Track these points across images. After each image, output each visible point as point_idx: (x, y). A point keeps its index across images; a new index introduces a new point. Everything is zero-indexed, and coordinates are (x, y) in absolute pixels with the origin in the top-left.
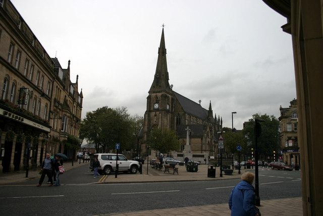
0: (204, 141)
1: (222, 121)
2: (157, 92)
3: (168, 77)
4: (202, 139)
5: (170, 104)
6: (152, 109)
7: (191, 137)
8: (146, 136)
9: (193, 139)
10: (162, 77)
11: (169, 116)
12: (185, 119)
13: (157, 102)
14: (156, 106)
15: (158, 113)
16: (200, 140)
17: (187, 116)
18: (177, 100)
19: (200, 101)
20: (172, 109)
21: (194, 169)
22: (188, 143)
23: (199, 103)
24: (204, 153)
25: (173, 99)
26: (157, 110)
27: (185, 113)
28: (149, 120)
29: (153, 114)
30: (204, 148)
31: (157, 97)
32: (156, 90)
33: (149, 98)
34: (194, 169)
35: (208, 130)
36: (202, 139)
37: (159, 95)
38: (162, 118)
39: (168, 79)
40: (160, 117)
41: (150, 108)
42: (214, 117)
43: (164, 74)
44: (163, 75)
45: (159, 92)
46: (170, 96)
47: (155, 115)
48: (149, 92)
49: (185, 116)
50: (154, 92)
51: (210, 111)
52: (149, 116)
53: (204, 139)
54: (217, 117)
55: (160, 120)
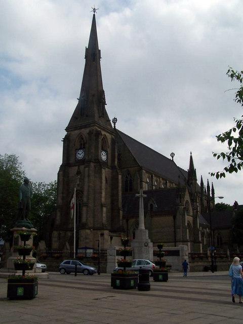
2: (81, 128)
3: (104, 99)
4: (175, 218)
5: (109, 150)
6: (72, 161)
7: (150, 213)
8: (59, 214)
9: (156, 219)
11: (105, 172)
12: (141, 181)
13: (82, 147)
14: (80, 155)
15: (82, 167)
16: (171, 218)
17: (146, 178)
18: (122, 142)
19: (173, 155)
20: (113, 161)
22: (142, 226)
23: (170, 158)
24: (180, 246)
25: (113, 142)
26: (82, 162)
27: (141, 169)
29: (73, 170)
30: (180, 236)
33: (66, 140)
35: (187, 197)
36: (175, 218)
37: (85, 131)
39: (104, 103)
40: (86, 174)
42: (199, 182)
44: (93, 96)
45: (85, 127)
46: (109, 136)
47: (78, 173)
48: (67, 129)
49: (141, 175)
50: (76, 129)
51: (192, 171)
53: (179, 217)
54: (205, 184)
55: (86, 179)
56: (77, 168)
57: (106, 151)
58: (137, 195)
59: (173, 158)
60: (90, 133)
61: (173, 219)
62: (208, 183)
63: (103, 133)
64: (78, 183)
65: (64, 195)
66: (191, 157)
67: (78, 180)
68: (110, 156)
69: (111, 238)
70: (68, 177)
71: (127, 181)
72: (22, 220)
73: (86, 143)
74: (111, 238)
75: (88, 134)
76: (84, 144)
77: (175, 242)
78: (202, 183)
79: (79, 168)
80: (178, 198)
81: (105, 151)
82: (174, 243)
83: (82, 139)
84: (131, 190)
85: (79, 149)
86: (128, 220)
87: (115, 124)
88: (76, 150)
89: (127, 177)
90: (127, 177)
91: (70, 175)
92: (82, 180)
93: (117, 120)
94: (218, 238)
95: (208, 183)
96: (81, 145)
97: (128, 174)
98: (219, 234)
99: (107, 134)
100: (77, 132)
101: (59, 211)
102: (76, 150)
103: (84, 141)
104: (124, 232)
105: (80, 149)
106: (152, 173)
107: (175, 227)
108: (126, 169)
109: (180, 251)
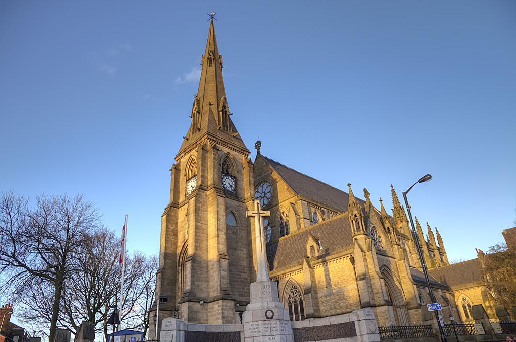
10: (206, 109)
43: (213, 101)
70: (177, 223)
81: (231, 176)
85: (191, 179)
87: (258, 150)
94: (464, 307)
99: (233, 153)
102: (187, 181)
109: (356, 323)
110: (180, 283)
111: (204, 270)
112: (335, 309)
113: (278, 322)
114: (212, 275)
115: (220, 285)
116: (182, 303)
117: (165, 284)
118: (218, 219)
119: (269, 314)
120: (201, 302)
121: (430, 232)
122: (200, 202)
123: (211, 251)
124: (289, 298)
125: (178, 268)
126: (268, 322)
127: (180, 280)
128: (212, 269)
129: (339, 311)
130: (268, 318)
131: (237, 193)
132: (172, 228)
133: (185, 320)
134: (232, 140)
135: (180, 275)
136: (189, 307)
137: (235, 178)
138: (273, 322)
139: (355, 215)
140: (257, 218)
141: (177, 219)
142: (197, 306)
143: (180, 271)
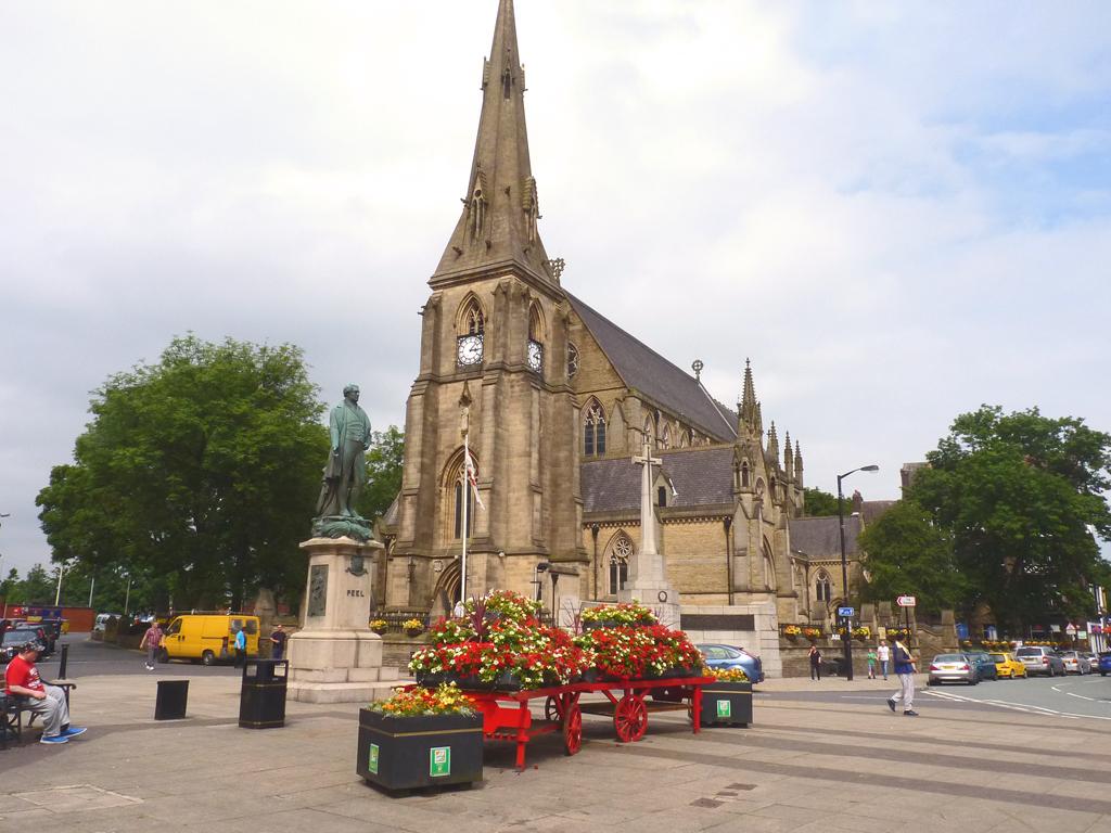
0: (740, 538)
1: (799, 460)
6: (446, 368)
10: (501, 199)
14: (470, 351)
15: (475, 385)
19: (698, 366)
21: (724, 707)
26: (477, 370)
28: (431, 429)
29: (448, 396)
31: (473, 302)
32: (470, 265)
33: (433, 310)
34: (724, 707)
38: (497, 407)
41: (436, 364)
42: (766, 440)
43: (512, 183)
45: (484, 276)
48: (435, 283)
50: (459, 281)
51: (750, 409)
52: (430, 404)
53: (739, 522)
56: (460, 385)
57: (541, 346)
58: (638, 459)
59: (698, 372)
60: (502, 292)
61: (722, 531)
62: (788, 440)
63: (534, 294)
64: (464, 426)
65: (426, 460)
66: (748, 371)
67: (465, 419)
68: (549, 357)
69: (555, 580)
70: (437, 411)
71: (590, 427)
72: (338, 514)
73: (487, 321)
74: (555, 580)
75: (495, 294)
76: (481, 323)
77: (732, 590)
78: (774, 442)
79: (466, 387)
80: (738, 471)
82: (726, 597)
83: (477, 308)
84: (601, 449)
85: (466, 336)
86: (598, 530)
88: (459, 338)
89: (590, 416)
90: (590, 416)
91: (442, 407)
92: (476, 419)
93: (563, 265)
94: (819, 587)
95: (788, 440)
96: (473, 324)
97: (595, 409)
98: (822, 576)
100: (462, 290)
101: (411, 503)
102: (459, 338)
103: (481, 313)
104: (587, 562)
105: (472, 334)
106: (657, 406)
107: (732, 551)
108: (587, 395)
110: (442, 514)
111: (504, 505)
112: (690, 585)
113: (671, 606)
114: (517, 515)
115: (532, 532)
116: (473, 553)
117: (421, 514)
118: (531, 428)
119: (663, 597)
120: (502, 554)
121: (788, 451)
122: (501, 393)
123: (515, 476)
124: (613, 557)
125: (438, 488)
126: (661, 605)
127: (443, 508)
128: (516, 505)
129: (694, 589)
130: (661, 601)
131: (542, 373)
132: (430, 419)
133: (480, 579)
134: (540, 272)
135: (443, 500)
136: (488, 561)
137: (542, 345)
138: (666, 605)
139: (745, 464)
140: (646, 467)
141: (437, 403)
142: (495, 560)
143: (443, 494)
